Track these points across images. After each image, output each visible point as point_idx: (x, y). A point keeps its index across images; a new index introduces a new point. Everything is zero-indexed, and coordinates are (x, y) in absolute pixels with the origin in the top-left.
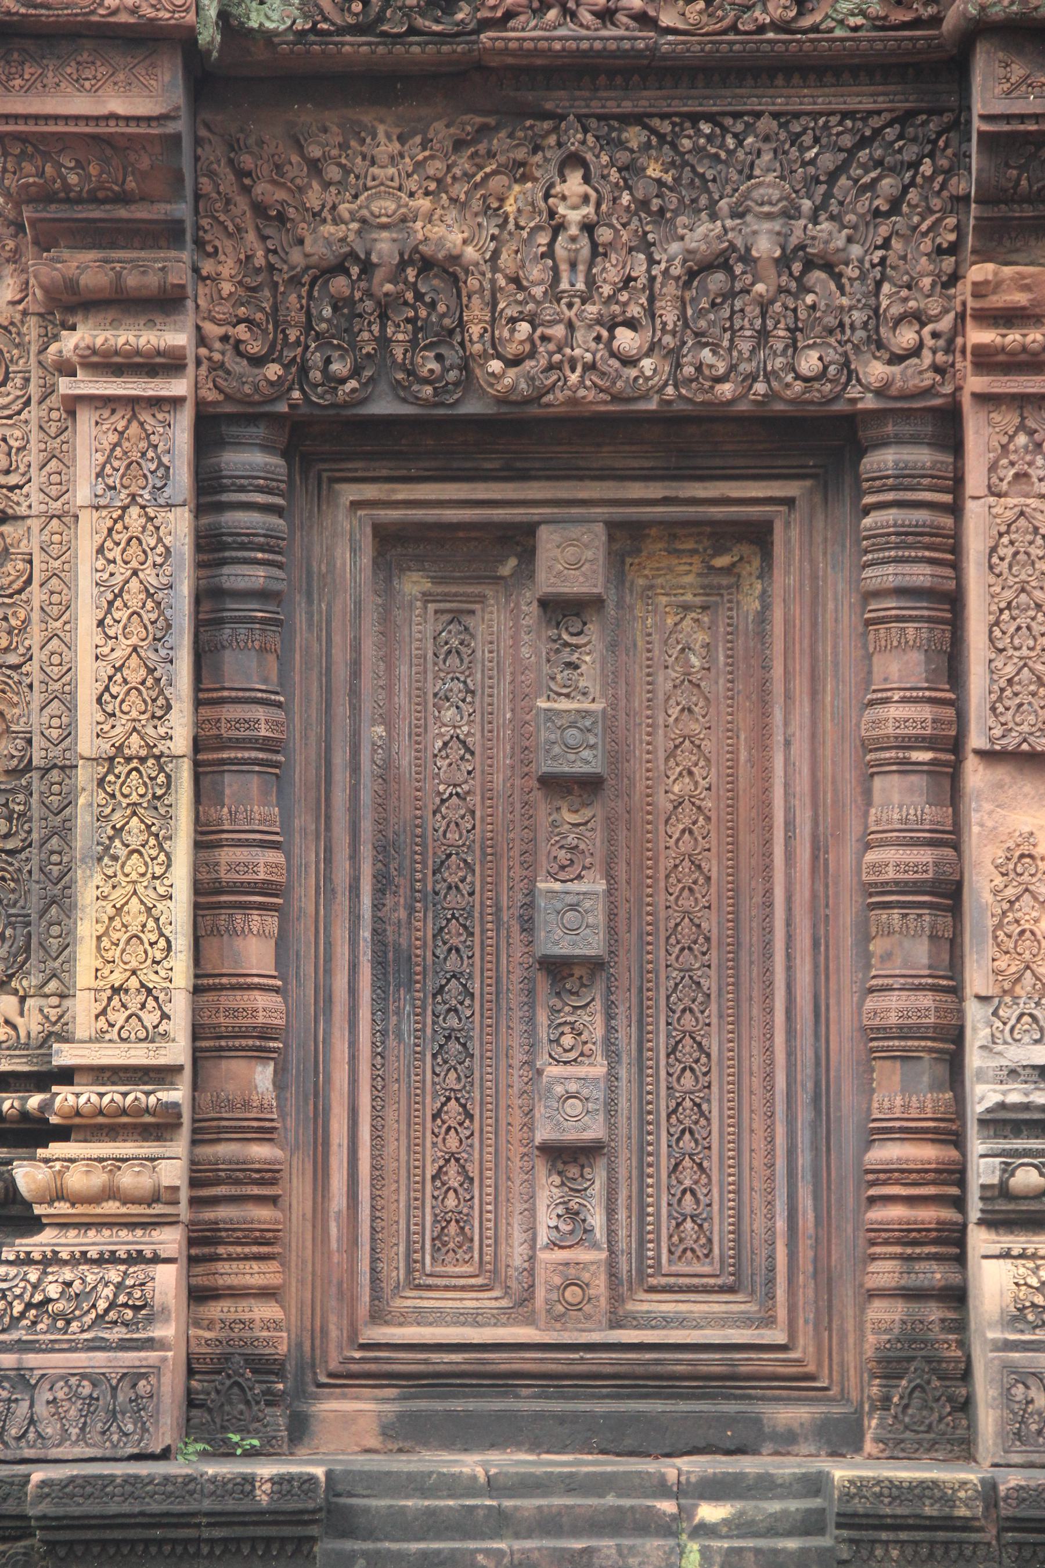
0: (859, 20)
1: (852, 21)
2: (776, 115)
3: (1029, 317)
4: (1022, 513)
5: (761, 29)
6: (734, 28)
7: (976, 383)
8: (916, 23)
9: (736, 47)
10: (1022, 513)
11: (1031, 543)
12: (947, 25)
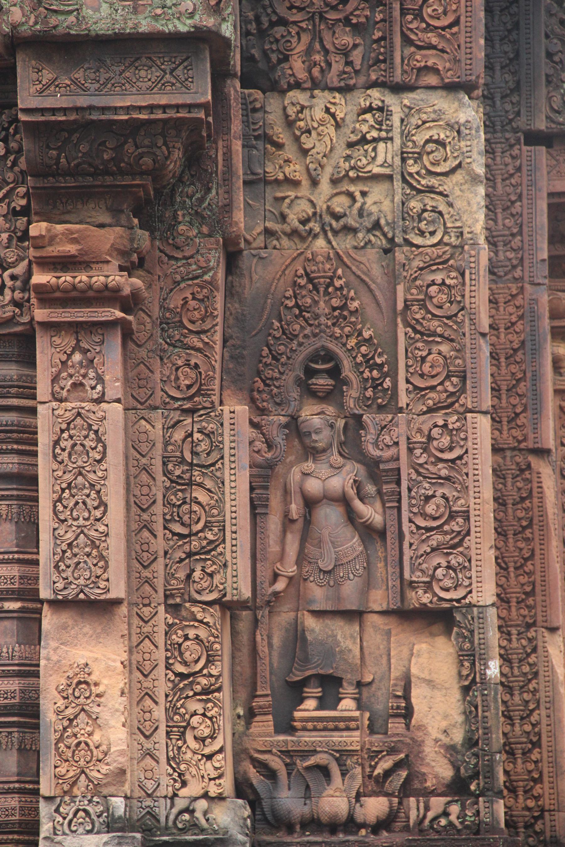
3: (80, 263)
4: (79, 414)
7: (41, 314)
10: (79, 414)
11: (86, 437)
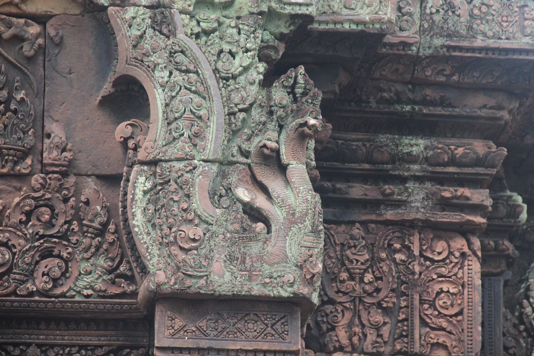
0: (90, 292)
1: (85, 292)
2: (39, 346)
5: (31, 294)
6: (14, 293)
8: (123, 295)
9: (15, 304)
12: (140, 297)
